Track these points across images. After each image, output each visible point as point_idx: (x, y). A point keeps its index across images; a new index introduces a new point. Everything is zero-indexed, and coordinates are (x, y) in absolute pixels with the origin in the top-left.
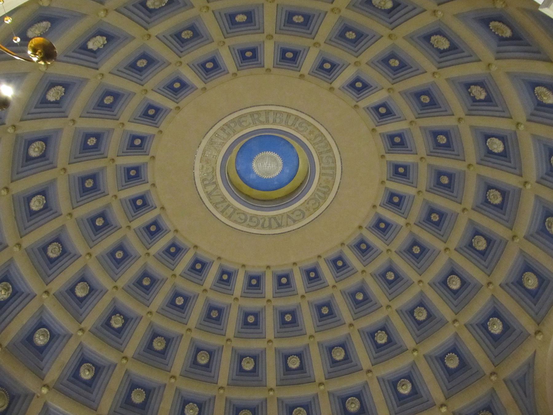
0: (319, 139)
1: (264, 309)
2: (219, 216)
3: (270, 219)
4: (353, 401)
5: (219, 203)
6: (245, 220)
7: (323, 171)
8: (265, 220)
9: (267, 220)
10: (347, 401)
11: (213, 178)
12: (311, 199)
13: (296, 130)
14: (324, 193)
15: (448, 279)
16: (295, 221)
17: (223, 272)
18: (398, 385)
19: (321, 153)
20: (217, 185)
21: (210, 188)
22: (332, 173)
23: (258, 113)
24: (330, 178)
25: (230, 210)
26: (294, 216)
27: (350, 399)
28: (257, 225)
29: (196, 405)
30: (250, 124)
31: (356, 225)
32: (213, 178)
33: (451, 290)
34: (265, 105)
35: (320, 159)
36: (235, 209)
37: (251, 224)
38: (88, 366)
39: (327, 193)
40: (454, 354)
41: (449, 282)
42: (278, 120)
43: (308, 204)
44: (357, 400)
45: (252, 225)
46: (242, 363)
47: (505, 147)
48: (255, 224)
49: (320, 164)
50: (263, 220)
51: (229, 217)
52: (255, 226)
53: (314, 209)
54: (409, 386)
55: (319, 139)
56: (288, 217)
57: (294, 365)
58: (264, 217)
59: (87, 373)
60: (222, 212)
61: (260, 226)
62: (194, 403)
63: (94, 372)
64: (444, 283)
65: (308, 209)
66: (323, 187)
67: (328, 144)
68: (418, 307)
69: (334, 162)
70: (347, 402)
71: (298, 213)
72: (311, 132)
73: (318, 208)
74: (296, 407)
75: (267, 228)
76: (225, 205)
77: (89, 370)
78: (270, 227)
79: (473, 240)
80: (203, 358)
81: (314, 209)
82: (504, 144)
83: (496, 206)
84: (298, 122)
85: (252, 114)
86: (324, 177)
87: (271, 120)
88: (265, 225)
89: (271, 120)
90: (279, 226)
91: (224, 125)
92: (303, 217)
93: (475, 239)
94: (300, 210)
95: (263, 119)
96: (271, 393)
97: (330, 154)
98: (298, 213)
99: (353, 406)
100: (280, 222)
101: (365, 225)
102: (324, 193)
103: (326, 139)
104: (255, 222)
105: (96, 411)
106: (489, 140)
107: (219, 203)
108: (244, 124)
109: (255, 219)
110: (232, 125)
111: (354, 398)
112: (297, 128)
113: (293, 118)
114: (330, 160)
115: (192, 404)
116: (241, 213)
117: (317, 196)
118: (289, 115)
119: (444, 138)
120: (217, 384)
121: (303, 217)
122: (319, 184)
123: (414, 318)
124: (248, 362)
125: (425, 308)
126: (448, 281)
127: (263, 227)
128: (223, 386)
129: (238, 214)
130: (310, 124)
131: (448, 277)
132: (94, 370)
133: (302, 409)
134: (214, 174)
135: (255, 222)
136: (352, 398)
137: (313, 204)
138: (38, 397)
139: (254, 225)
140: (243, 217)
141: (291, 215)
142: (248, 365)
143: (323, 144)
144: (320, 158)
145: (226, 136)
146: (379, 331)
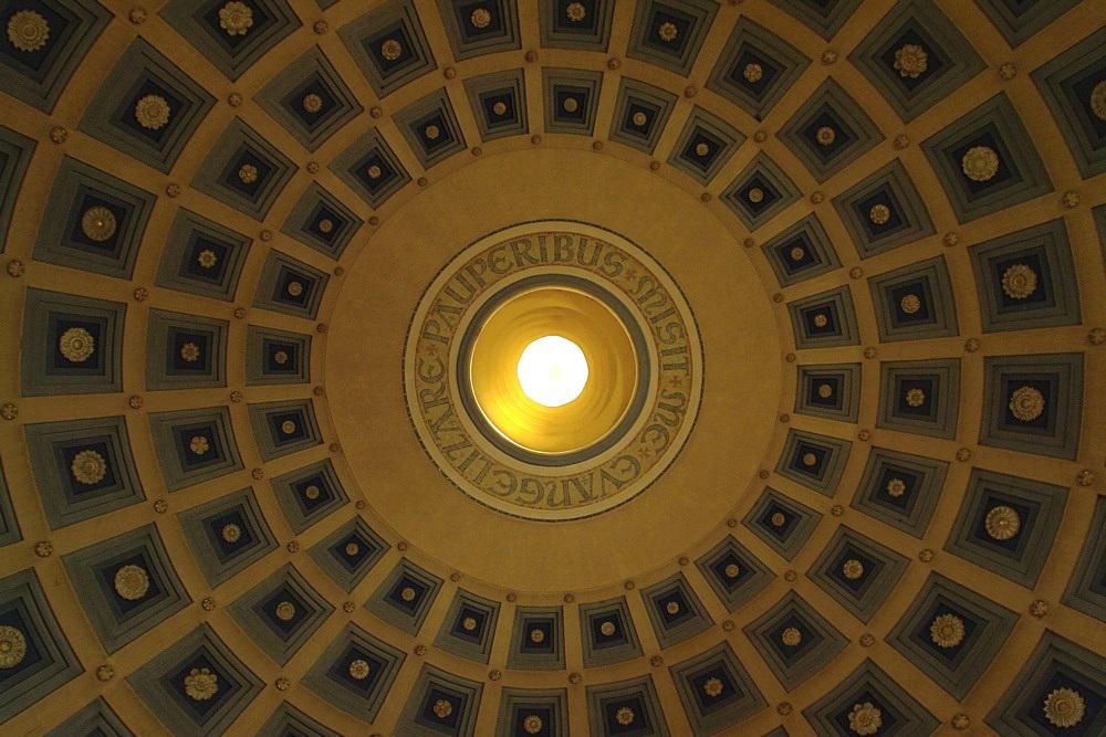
0: (647, 287)
1: (562, 697)
2: (454, 476)
3: (565, 484)
5: (455, 447)
6: (513, 487)
7: (667, 360)
8: (555, 486)
9: (560, 485)
11: (442, 389)
12: (649, 429)
13: (601, 272)
14: (674, 410)
15: (987, 521)
16: (619, 485)
17: (466, 612)
19: (655, 320)
20: (451, 406)
21: (437, 412)
22: (684, 361)
23: (525, 240)
24: (681, 373)
25: (476, 467)
26: (615, 474)
28: (539, 499)
30: (511, 265)
31: (753, 469)
32: (442, 389)
33: (1001, 543)
34: (538, 221)
35: (656, 333)
36: (490, 463)
37: (523, 496)
39: (679, 411)
40: (1062, 690)
41: (993, 532)
42: (564, 255)
43: (643, 441)
45: (526, 500)
47: (1000, 159)
48: (532, 498)
49: (657, 345)
50: (551, 487)
51: (477, 482)
52: (534, 503)
53: (658, 451)
55: (647, 287)
56: (605, 475)
58: (552, 481)
60: (461, 469)
61: (545, 499)
64: (980, 534)
65: (645, 453)
66: (670, 397)
67: (667, 297)
68: (938, 619)
69: (684, 334)
71: (625, 464)
72: (630, 275)
73: (665, 448)
75: (562, 506)
76: (468, 452)
78: (567, 502)
79: (1011, 407)
81: (658, 451)
82: (996, 151)
83: (1031, 299)
84: (603, 254)
85: (514, 243)
86: (670, 374)
87: (551, 256)
88: (559, 497)
89: (551, 256)
90: (587, 498)
91: (461, 269)
92: (637, 473)
93: (1014, 403)
94: (627, 457)
95: (535, 253)
97: (673, 318)
98: (625, 464)
100: (587, 488)
101: (771, 467)
102: (674, 410)
103: (660, 286)
104: (533, 492)
106: (965, 159)
107: (455, 447)
108: (499, 265)
109: (532, 486)
110: (477, 268)
112: (602, 269)
113: (591, 245)
114: (675, 331)
116: (504, 472)
117: (660, 421)
118: (584, 239)
119: (883, 208)
121: (637, 473)
122: (662, 391)
123: (935, 645)
125: (954, 614)
126: (988, 527)
127: (552, 504)
129: (496, 473)
130: (624, 256)
131: (984, 517)
134: (444, 380)
135: (533, 492)
137: (654, 441)
139: (532, 500)
140: (507, 480)
141: (611, 472)
143: (656, 298)
144: (655, 331)
145: (466, 294)
146: (857, 706)
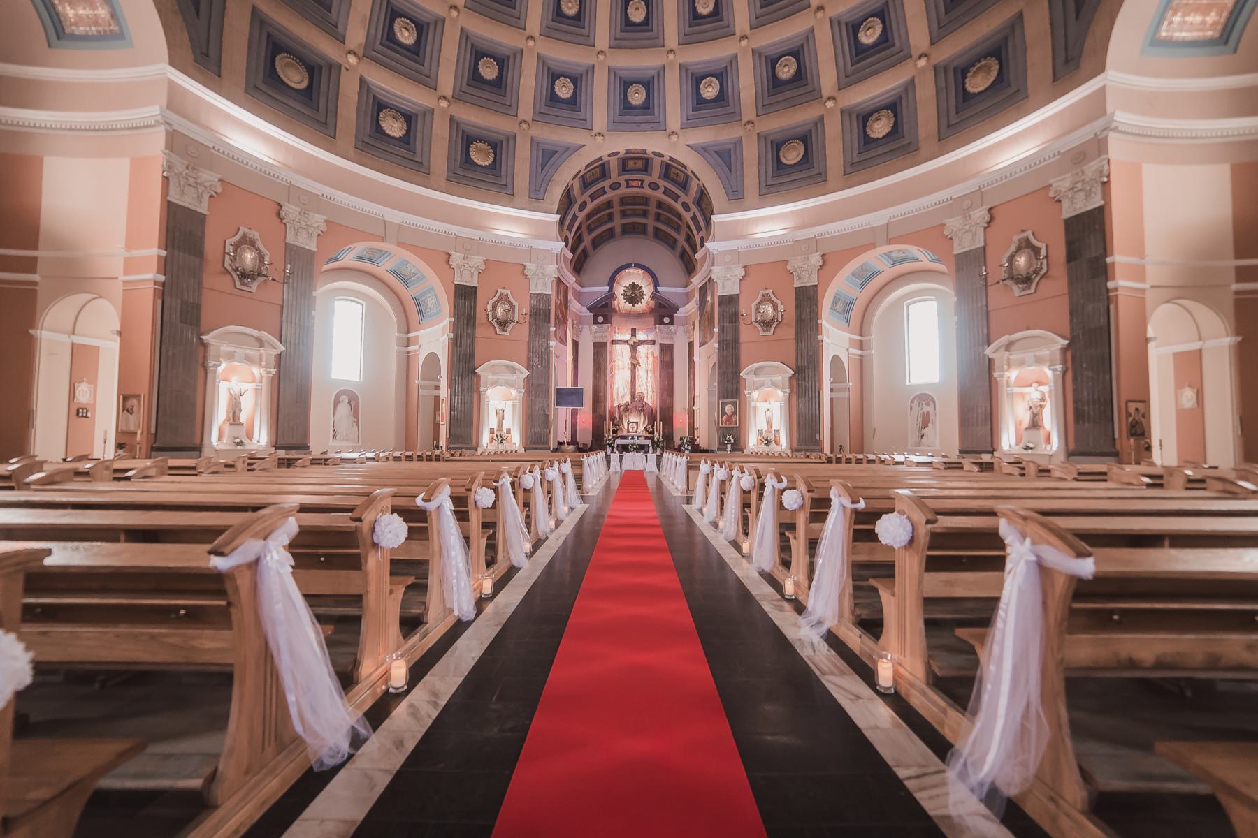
4: (788, 63)
10: (779, 63)
18: (861, 30)
27: (783, 59)
29: (569, 80)
38: (403, 22)
44: (794, 59)
46: (629, 11)
54: (879, 29)
57: (705, 8)
59: (406, 34)
62: (566, 77)
63: (415, 32)
70: (777, 66)
74: (705, 77)
77: (407, 29)
80: (570, 5)
96: (671, 56)
99: (786, 69)
105: (436, 90)
111: (790, 57)
115: (563, 78)
120: (594, 46)
124: (637, 9)
128: (603, 49)
132: (415, 29)
133: (714, 79)
136: (787, 57)
138: (347, 69)
142: (637, 12)
